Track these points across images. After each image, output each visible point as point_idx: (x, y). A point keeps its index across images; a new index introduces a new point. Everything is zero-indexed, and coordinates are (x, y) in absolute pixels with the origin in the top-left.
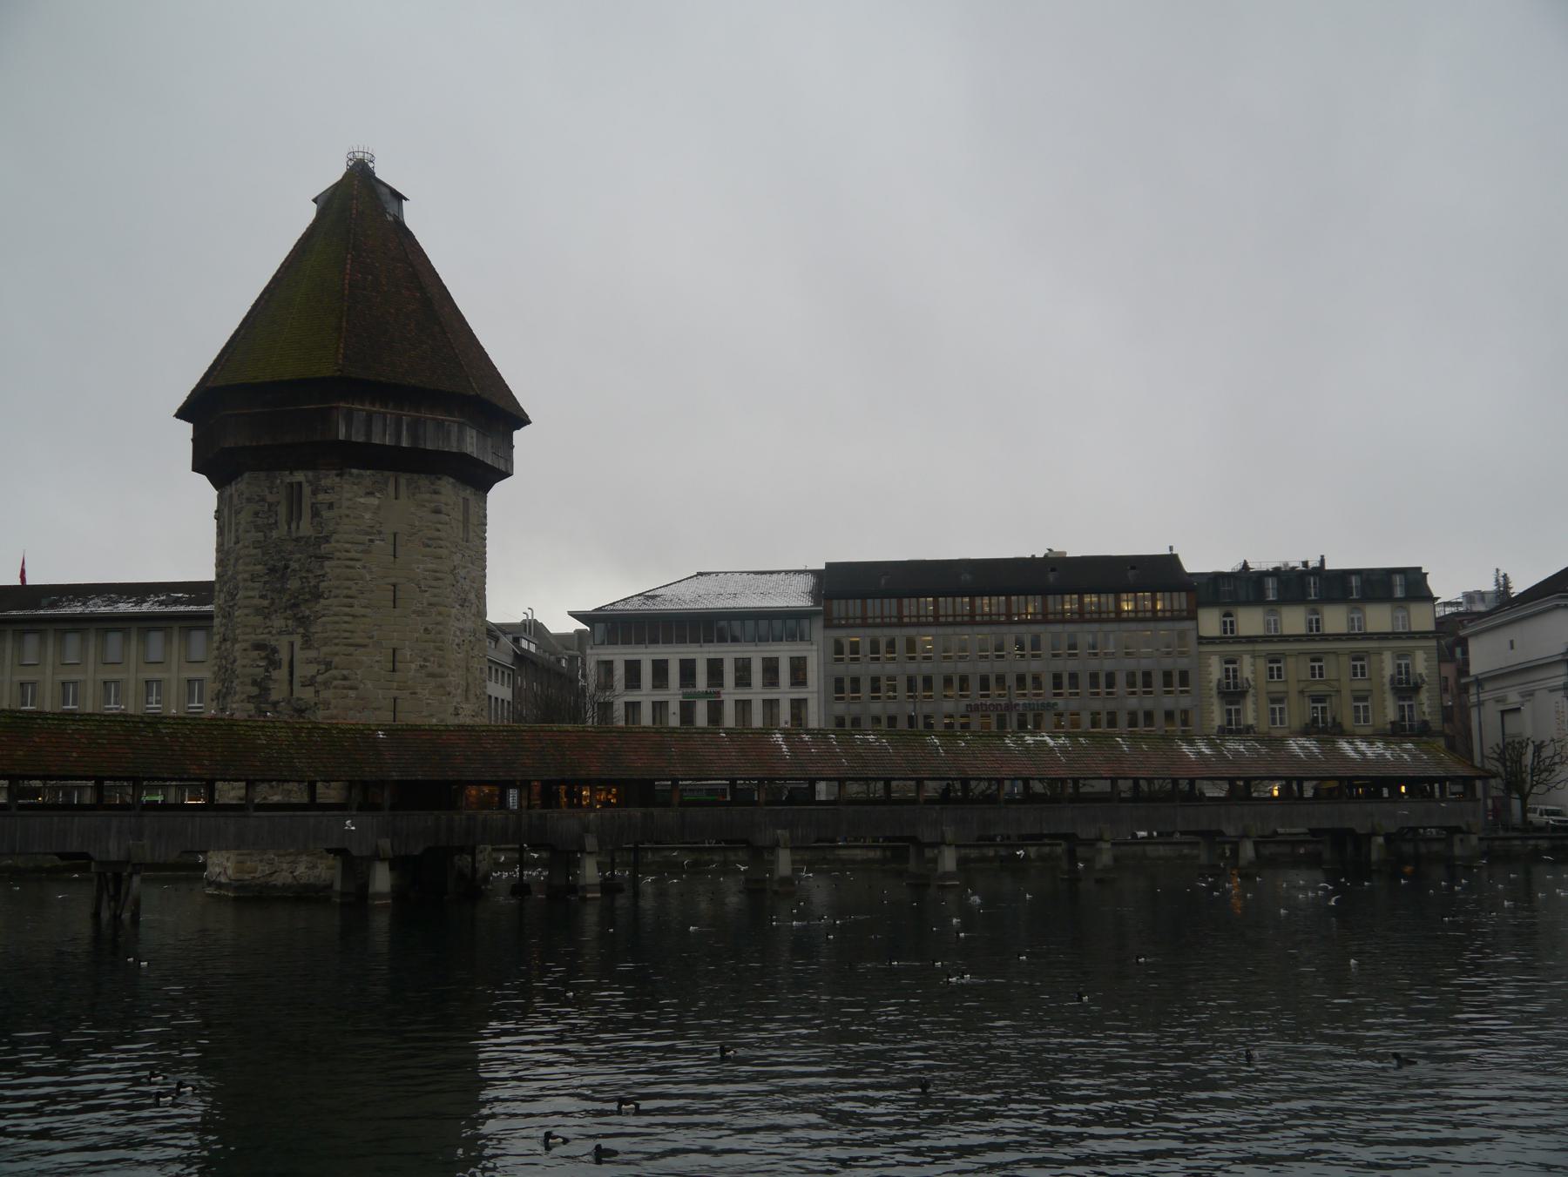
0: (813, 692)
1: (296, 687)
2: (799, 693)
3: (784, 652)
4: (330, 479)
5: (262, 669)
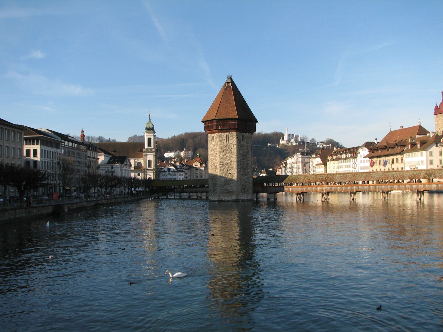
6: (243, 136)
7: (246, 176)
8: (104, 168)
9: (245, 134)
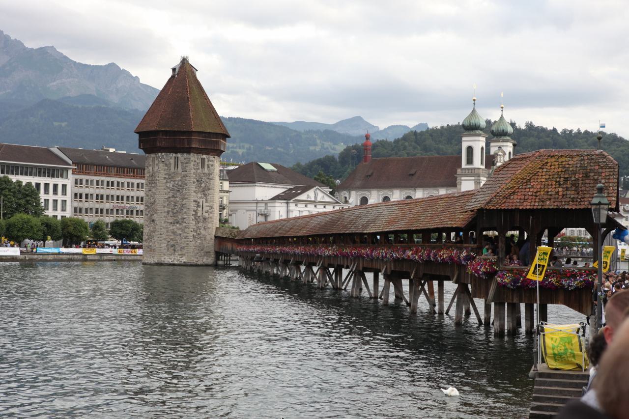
0: (69, 198)
1: (204, 213)
2: (64, 198)
3: (60, 181)
4: (211, 158)
5: (195, 208)
6: (177, 159)
7: (178, 225)
8: (255, 208)
9: (179, 155)
